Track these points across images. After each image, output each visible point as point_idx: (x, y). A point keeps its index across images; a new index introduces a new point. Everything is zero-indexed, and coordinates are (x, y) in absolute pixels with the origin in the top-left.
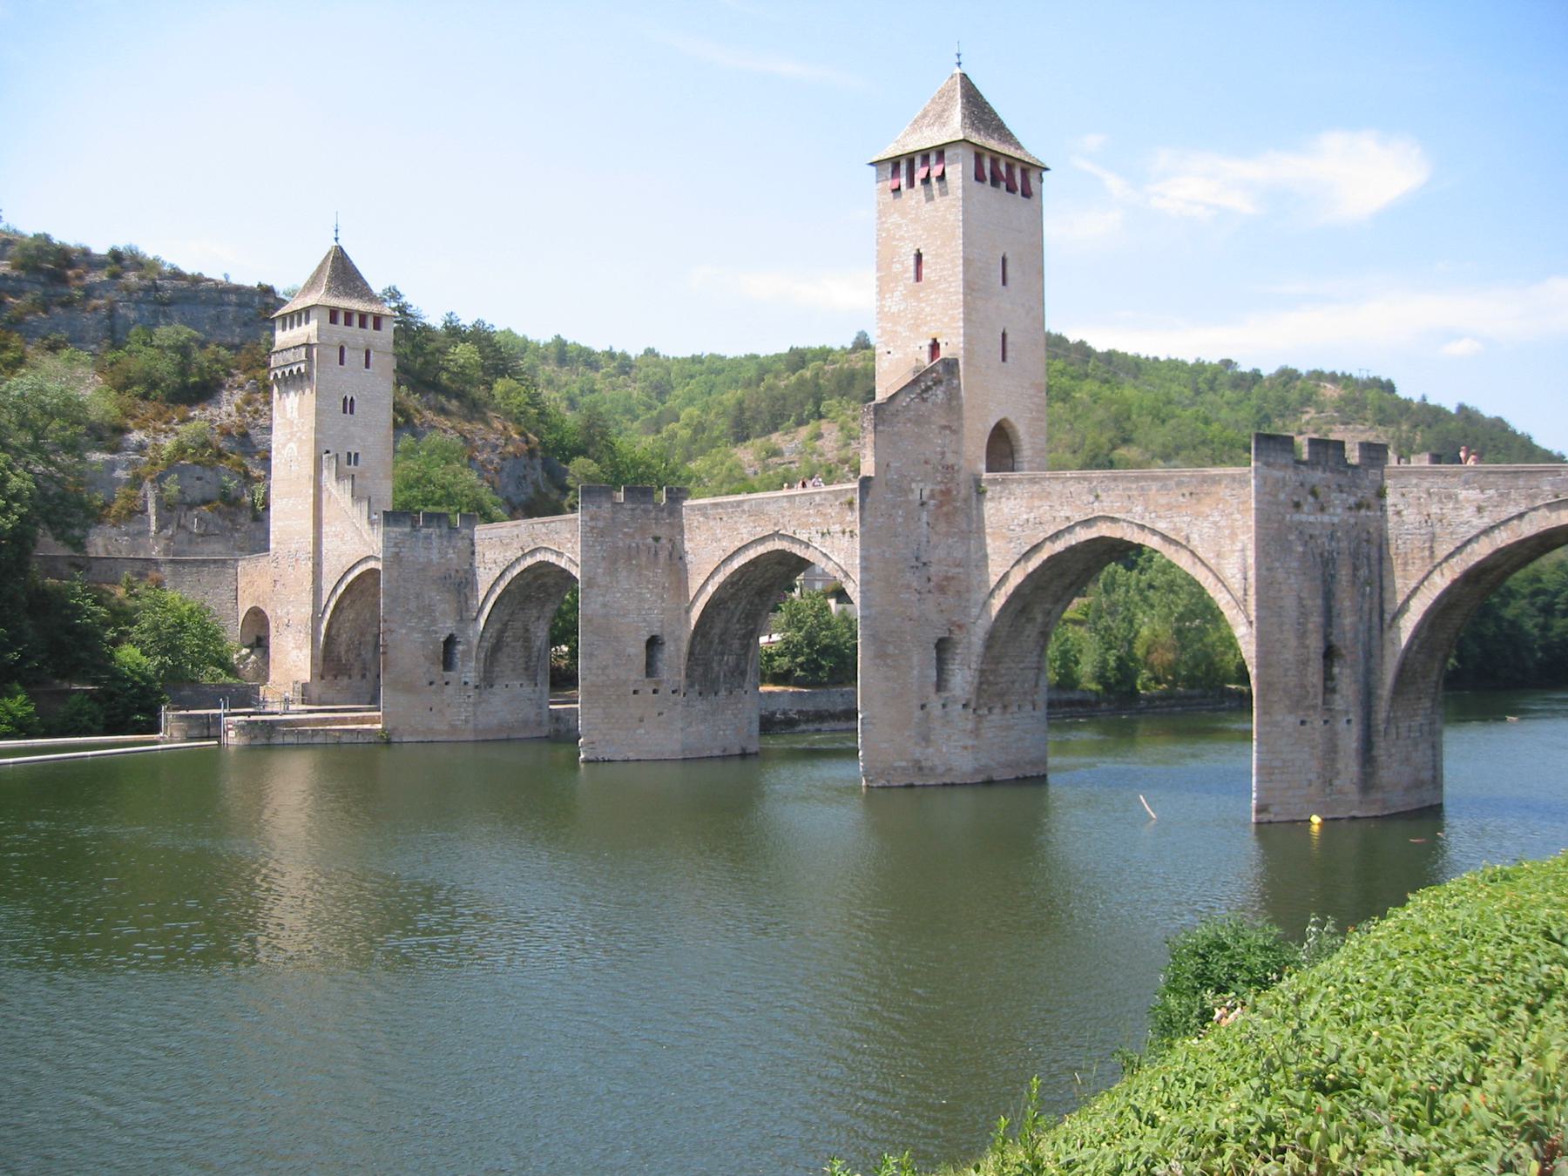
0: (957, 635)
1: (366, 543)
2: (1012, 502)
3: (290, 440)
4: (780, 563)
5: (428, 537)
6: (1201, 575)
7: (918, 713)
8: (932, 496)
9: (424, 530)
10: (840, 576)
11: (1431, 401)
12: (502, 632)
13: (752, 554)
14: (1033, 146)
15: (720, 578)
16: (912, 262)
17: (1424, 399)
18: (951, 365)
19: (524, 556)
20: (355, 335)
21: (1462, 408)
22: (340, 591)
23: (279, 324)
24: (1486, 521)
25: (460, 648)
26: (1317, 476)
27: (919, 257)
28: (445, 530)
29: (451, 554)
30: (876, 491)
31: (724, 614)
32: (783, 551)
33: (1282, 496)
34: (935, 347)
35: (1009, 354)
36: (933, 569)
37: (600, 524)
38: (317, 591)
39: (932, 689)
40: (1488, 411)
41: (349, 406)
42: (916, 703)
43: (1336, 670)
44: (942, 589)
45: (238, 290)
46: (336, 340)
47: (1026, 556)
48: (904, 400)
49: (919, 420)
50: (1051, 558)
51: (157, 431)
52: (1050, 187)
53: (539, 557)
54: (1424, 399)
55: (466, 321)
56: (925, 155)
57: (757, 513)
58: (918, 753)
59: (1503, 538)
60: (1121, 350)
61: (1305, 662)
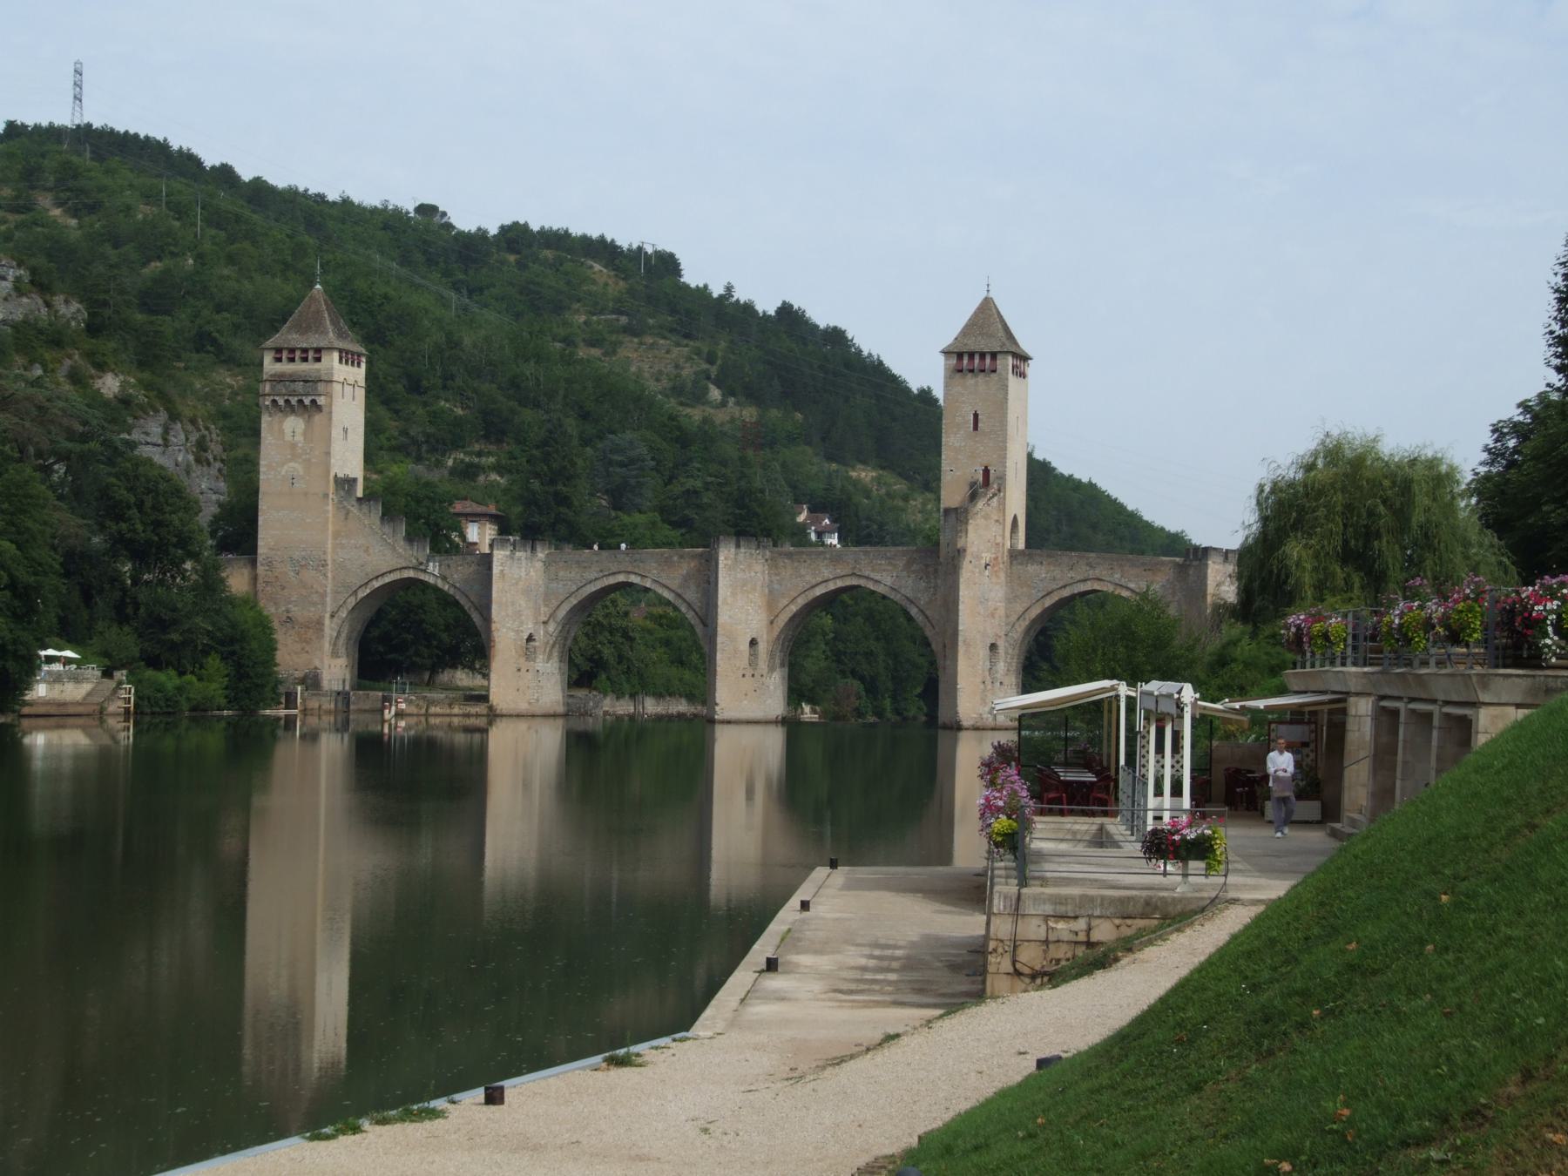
1: (400, 556)
10: (904, 603)
11: (741, 295)
14: (1025, 345)
15: (801, 602)
17: (729, 289)
21: (786, 311)
22: (361, 594)
27: (976, 416)
34: (986, 472)
40: (822, 317)
41: (345, 431)
42: (979, 680)
49: (986, 517)
52: (1031, 369)
53: (621, 578)
54: (729, 289)
60: (1054, 464)
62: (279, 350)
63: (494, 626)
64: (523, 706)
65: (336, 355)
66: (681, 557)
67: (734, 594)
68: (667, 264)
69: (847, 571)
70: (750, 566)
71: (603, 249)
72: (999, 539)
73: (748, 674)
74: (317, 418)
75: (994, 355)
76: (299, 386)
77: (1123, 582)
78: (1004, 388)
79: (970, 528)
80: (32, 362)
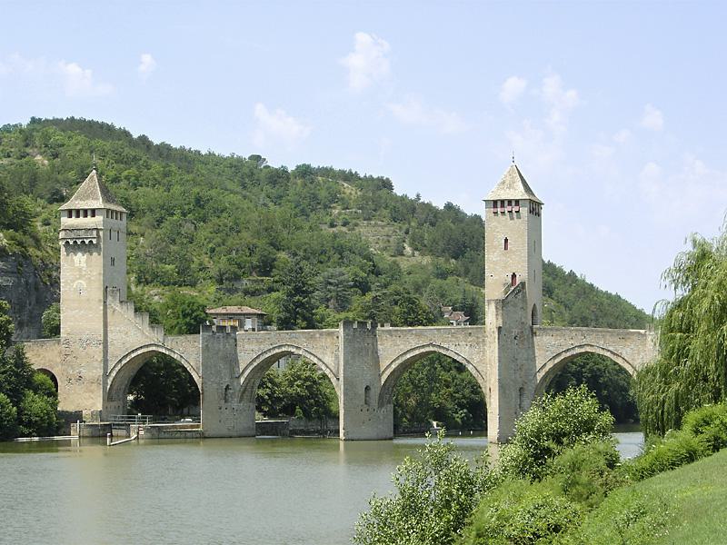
2: (548, 337)
3: (79, 279)
10: (464, 362)
14: (539, 196)
16: (503, 241)
18: (523, 284)
19: (274, 348)
21: (449, 207)
22: (124, 362)
27: (506, 240)
30: (503, 333)
34: (514, 276)
36: (518, 362)
38: (105, 361)
41: (113, 260)
47: (554, 357)
49: (515, 305)
53: (284, 349)
56: (510, 202)
57: (419, 335)
62: (70, 213)
66: (321, 334)
68: (386, 184)
71: (350, 177)
73: (365, 410)
76: (81, 233)
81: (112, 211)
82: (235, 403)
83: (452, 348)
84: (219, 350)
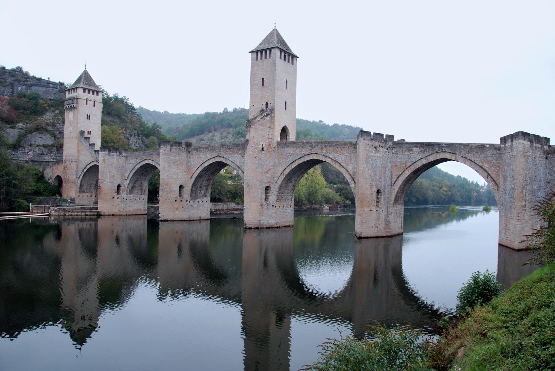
0: (271, 186)
1: (93, 157)
2: (288, 149)
4: (218, 165)
5: (113, 155)
6: (342, 170)
7: (260, 207)
8: (265, 146)
9: (112, 154)
12: (135, 183)
13: (211, 162)
14: (294, 51)
15: (200, 169)
16: (261, 80)
20: (91, 97)
22: (85, 171)
23: (67, 92)
24: (421, 157)
25: (122, 188)
26: (376, 144)
27: (263, 79)
28: (118, 153)
29: (120, 161)
31: (202, 179)
32: (220, 162)
33: (367, 148)
34: (267, 104)
35: (287, 108)
36: (265, 167)
37: (167, 152)
38: (77, 171)
39: (264, 201)
41: (88, 117)
42: (259, 204)
43: (379, 196)
44: (267, 173)
45: (53, 83)
46: (85, 98)
48: (257, 119)
49: (262, 125)
50: (299, 165)
51: (27, 123)
52: (299, 62)
53: (146, 162)
55: (120, 97)
58: (259, 218)
59: (424, 162)
61: (372, 194)
63: (99, 181)
64: (116, 211)
65: (80, 91)
67: (169, 166)
69: (216, 155)
70: (179, 154)
72: (271, 136)
74: (76, 111)
75: (270, 50)
76: (70, 101)
77: (327, 155)
78: (274, 64)
79: (251, 130)
80: (55, 110)
81: (89, 90)
82: (124, 194)
83: (230, 158)
84: (113, 163)
